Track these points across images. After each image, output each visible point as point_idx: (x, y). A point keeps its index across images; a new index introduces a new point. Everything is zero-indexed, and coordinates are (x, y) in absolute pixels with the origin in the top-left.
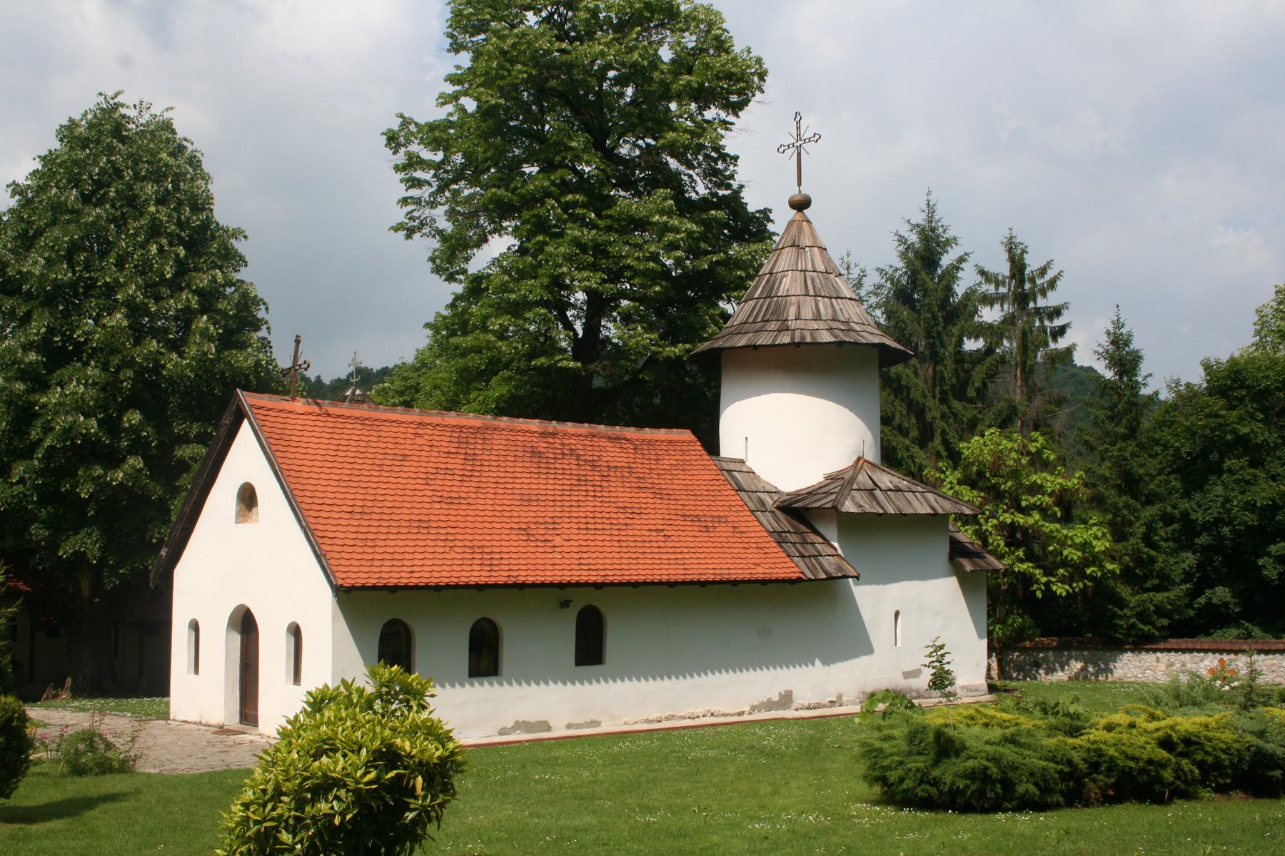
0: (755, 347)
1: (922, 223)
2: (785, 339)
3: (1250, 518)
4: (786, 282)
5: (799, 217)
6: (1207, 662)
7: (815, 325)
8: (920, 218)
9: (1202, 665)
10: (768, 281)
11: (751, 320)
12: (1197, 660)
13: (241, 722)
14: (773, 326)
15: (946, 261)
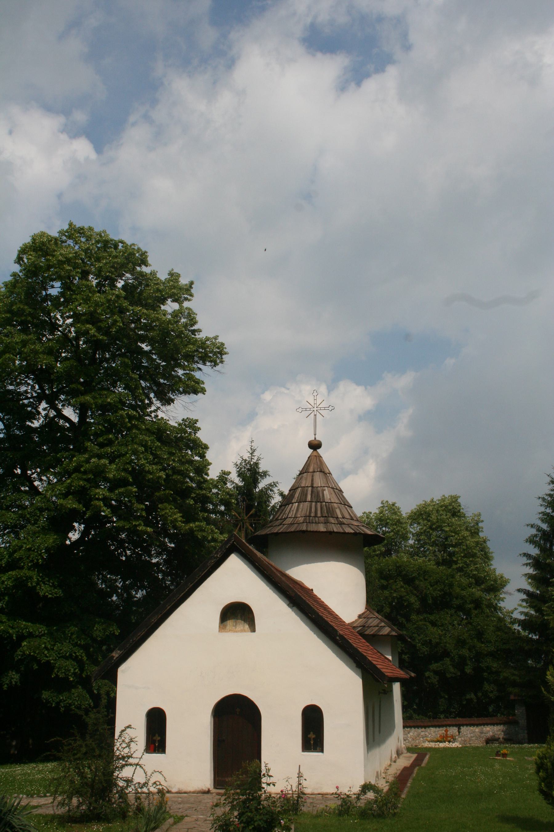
0: (331, 533)
1: (247, 459)
2: (348, 530)
3: (425, 649)
4: (326, 493)
5: (315, 453)
6: (411, 734)
7: (356, 523)
8: (247, 456)
9: (409, 735)
10: (312, 492)
11: (313, 515)
12: (407, 733)
13: (215, 787)
14: (332, 520)
15: (262, 484)
